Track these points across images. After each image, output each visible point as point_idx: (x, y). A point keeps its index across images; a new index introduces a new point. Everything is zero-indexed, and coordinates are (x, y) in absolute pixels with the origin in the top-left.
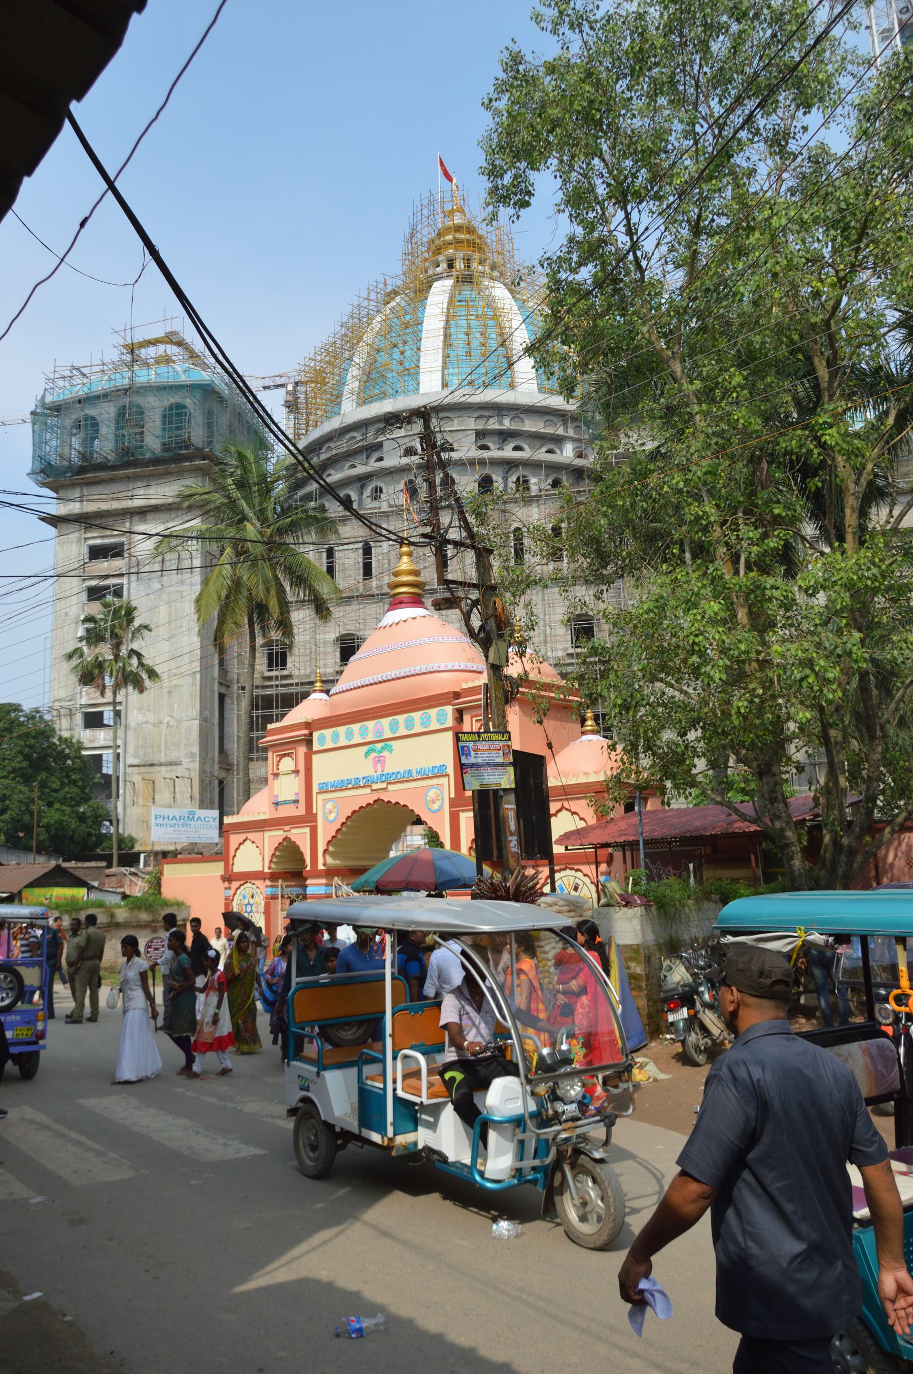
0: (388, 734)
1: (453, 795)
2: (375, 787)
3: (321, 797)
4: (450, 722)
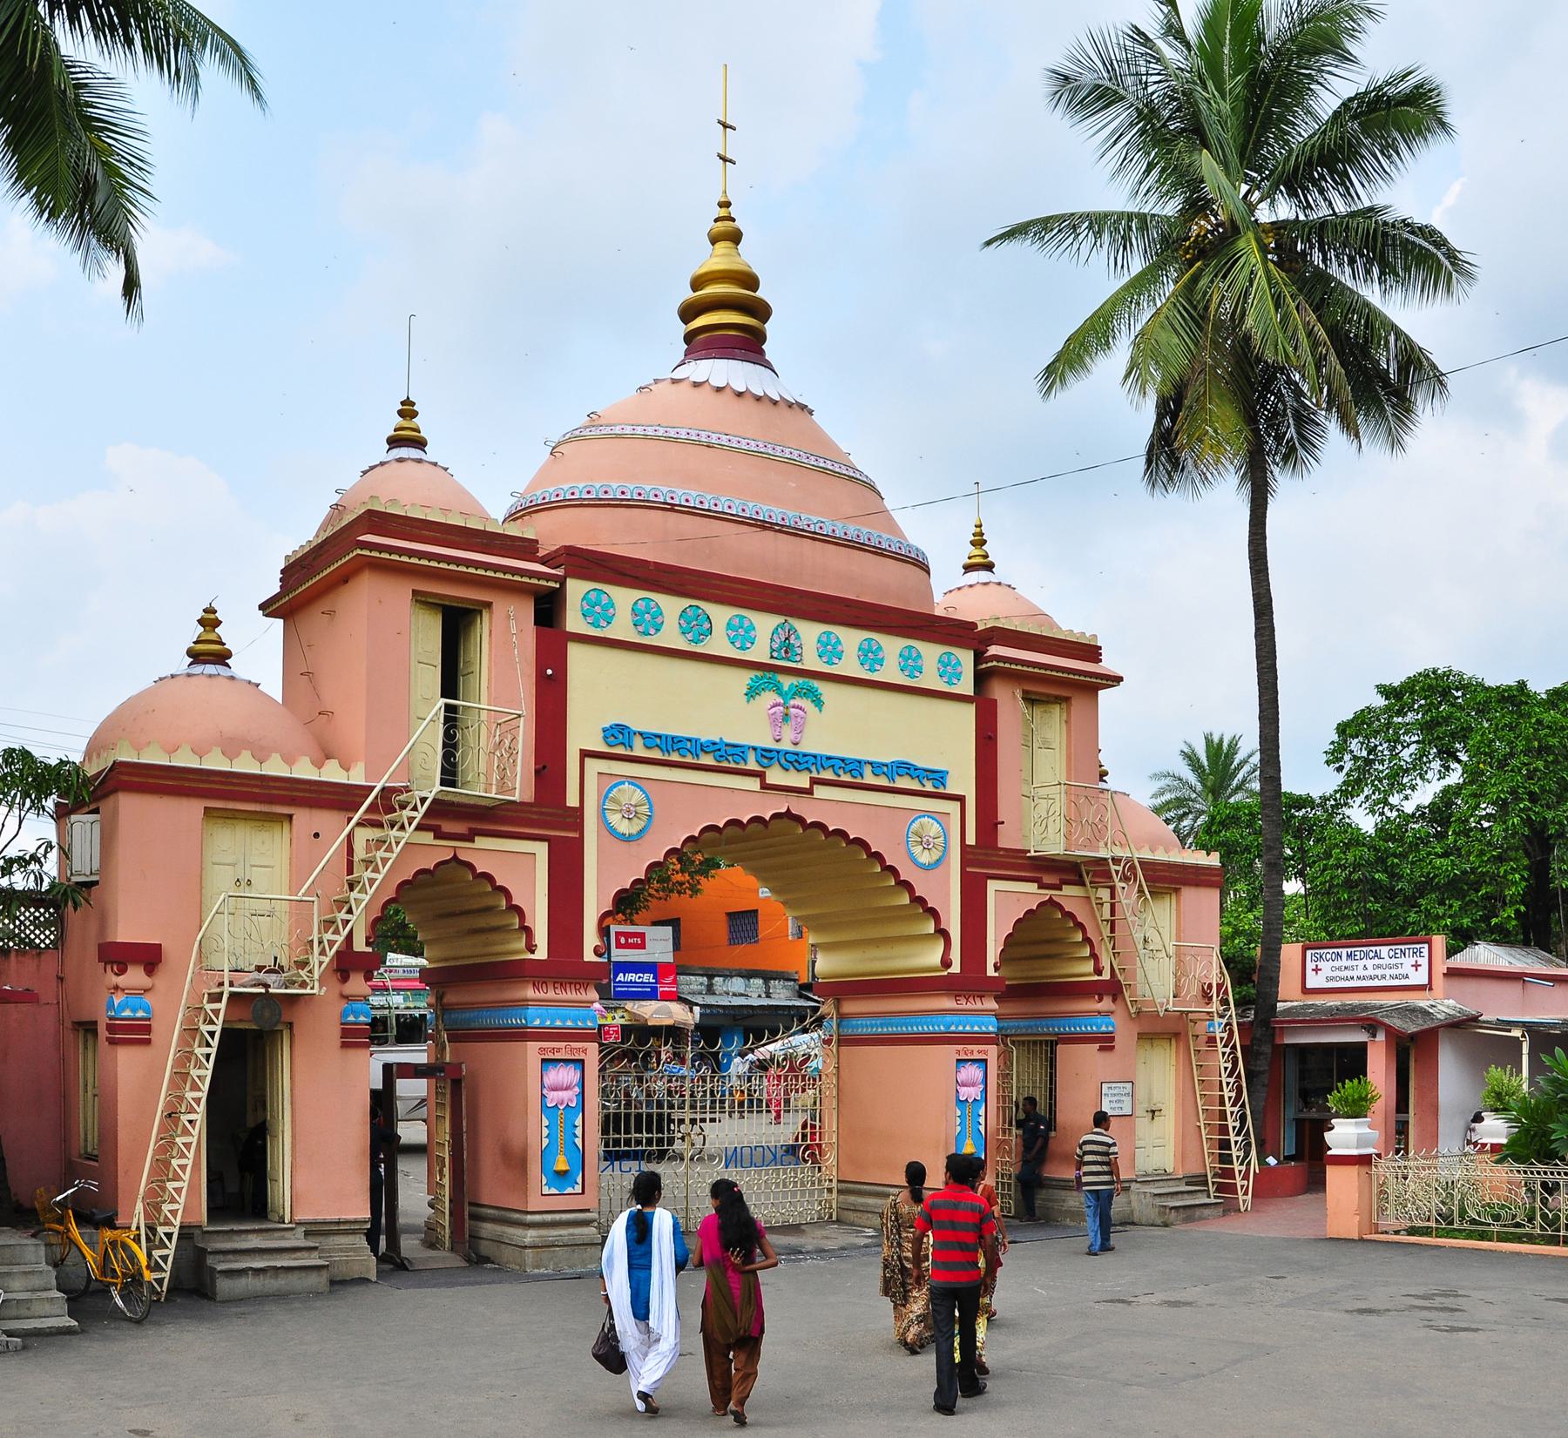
0: (811, 662)
1: (971, 840)
2: (775, 776)
3: (593, 766)
4: (966, 686)
